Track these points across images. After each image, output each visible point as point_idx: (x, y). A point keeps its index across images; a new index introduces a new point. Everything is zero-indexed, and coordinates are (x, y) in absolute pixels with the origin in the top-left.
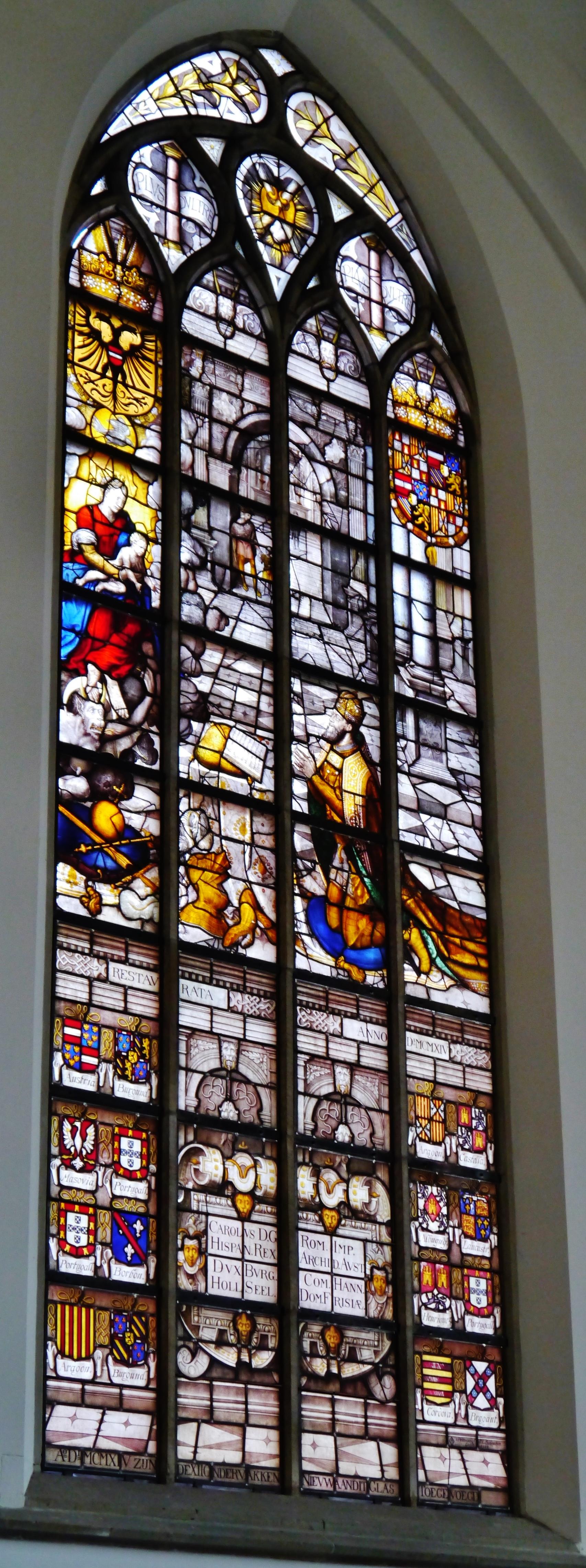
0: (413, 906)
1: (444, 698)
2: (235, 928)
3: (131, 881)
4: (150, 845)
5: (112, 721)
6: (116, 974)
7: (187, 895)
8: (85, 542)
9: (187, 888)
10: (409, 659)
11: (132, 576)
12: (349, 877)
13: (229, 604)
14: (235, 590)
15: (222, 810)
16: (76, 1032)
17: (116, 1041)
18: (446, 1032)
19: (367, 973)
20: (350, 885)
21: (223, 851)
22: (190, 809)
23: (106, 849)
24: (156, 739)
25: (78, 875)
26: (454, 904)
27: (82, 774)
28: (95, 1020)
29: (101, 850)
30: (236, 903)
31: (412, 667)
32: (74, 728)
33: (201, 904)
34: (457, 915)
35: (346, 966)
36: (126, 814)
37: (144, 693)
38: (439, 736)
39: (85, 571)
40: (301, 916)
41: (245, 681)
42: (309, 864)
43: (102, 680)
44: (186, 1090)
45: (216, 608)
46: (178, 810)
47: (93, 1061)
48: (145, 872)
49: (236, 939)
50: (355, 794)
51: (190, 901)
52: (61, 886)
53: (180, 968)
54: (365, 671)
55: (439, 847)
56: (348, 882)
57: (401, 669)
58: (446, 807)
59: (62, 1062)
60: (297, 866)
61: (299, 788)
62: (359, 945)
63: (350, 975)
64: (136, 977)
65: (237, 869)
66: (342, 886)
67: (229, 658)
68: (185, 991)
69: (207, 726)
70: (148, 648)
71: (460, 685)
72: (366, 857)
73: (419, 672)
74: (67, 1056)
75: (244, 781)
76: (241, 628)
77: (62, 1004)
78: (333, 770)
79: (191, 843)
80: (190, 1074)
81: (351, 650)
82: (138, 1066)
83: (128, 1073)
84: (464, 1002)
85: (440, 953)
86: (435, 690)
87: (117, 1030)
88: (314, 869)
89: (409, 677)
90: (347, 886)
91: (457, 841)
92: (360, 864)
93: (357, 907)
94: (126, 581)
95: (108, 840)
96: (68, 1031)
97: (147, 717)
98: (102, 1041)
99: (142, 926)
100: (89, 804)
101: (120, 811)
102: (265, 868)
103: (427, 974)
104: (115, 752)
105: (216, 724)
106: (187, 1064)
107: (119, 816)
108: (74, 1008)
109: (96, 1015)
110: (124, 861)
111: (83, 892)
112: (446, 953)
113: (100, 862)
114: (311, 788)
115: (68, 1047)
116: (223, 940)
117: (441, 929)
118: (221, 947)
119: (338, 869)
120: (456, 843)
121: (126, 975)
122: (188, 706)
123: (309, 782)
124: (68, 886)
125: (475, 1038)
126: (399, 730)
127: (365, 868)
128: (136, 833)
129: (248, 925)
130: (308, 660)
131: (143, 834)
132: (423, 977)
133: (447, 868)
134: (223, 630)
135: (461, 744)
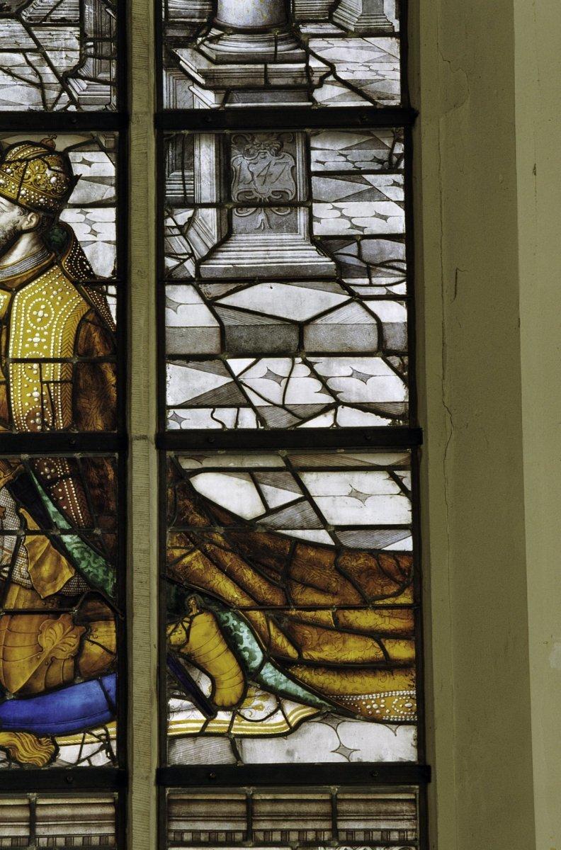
0: (198, 566)
12: (19, 543)
18: (286, 826)
19: (60, 741)
20: (21, 561)
26: (323, 537)
31: (217, 39)
34: (327, 559)
38: (287, 175)
50: (40, 361)
54: (78, 86)
55: (279, 421)
57: (185, 55)
58: (301, 327)
62: (40, 685)
63: (10, 758)
71: (354, 42)
72: (69, 489)
81: (39, 49)
84: (341, 749)
86: (280, 74)
89: (205, 65)
90: (12, 565)
91: (333, 393)
92: (52, 508)
93: (38, 605)
103: (235, 708)
112: (291, 651)
117: (278, 600)
120: (331, 400)
125: (371, 825)
127: (65, 515)
132: (223, 716)
133: (303, 461)
135: (354, 175)
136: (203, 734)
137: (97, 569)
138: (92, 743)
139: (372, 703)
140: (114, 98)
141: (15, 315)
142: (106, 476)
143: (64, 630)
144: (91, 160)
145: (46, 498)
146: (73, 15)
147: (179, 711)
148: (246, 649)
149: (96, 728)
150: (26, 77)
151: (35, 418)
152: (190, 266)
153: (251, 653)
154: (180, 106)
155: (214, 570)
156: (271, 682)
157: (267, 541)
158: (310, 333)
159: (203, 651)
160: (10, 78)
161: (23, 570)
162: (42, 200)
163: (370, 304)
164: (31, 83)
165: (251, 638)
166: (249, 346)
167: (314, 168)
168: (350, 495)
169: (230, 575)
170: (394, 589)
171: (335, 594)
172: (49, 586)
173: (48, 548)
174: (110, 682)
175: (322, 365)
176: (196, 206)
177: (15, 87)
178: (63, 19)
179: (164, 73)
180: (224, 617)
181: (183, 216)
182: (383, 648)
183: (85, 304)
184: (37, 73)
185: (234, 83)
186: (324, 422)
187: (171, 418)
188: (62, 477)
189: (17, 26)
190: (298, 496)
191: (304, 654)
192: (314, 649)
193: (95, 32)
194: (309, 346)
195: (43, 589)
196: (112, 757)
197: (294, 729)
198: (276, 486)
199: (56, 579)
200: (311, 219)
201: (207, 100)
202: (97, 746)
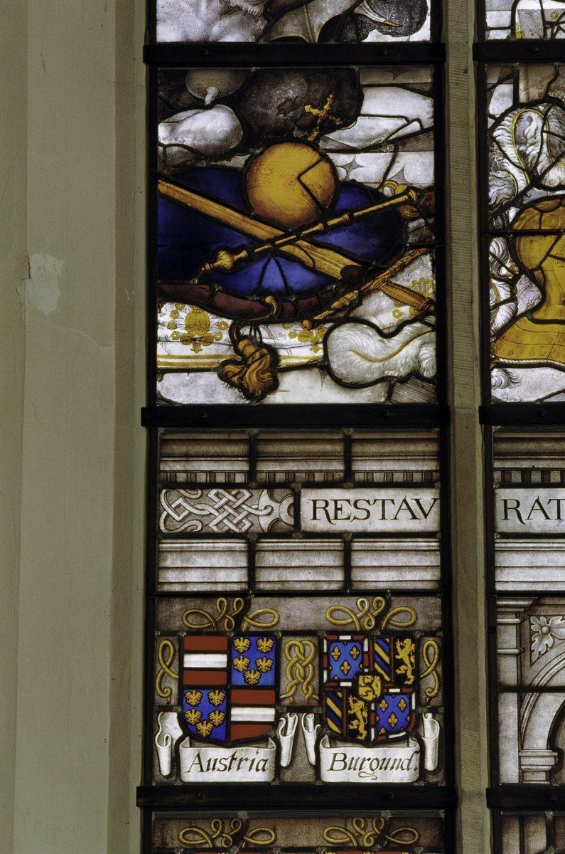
3: (359, 302)
4: (407, 212)
6: (321, 513)
7: (513, 298)
9: (511, 283)
16: (218, 661)
17: (323, 659)
22: (517, 104)
23: (285, 248)
25: (214, 320)
27: (218, 101)
28: (265, 623)
29: (274, 252)
33: (551, 312)
36: (341, 159)
44: (522, 737)
47: (267, 714)
48: (394, 275)
51: (522, 308)
52: (170, 351)
53: (497, 464)
59: (178, 733)
64: (376, 510)
68: (512, 515)
74: (192, 717)
77: (177, 606)
79: (522, 181)
80: (530, 698)
82: (383, 704)
83: (359, 725)
87: (323, 637)
95: (292, 229)
96: (192, 661)
98: (286, 666)
99: (390, 393)
100: (239, 161)
101: (324, 157)
104: (307, 28)
106: (520, 677)
107: (325, 166)
108: (208, 608)
109: (263, 613)
113: (273, 278)
115: (193, 697)
121: (348, 509)
124: (187, 350)
128: (367, 193)
131: (387, 191)
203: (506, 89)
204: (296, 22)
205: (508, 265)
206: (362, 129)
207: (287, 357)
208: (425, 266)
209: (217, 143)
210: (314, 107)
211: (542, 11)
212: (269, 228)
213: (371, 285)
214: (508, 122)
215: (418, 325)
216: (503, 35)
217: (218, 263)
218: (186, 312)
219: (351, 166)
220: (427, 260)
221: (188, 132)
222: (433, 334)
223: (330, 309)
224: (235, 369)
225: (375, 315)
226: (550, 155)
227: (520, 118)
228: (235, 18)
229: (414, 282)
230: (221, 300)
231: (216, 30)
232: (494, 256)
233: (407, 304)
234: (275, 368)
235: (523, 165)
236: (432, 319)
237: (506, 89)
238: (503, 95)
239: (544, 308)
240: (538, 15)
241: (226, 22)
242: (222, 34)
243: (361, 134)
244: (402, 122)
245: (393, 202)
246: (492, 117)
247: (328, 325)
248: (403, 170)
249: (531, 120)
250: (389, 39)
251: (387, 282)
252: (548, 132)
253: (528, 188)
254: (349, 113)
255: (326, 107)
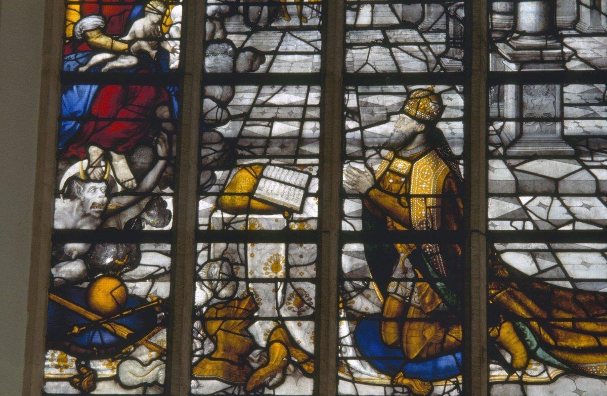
1: (562, 59)
2: (261, 370)
4: (157, 309)
5: (117, 194)
7: (202, 348)
8: (90, 28)
9: (202, 341)
10: (513, 31)
11: (144, 45)
12: (413, 286)
13: (267, 41)
14: (273, 25)
15: (249, 252)
19: (434, 384)
20: (415, 295)
21: (250, 294)
22: (209, 260)
24: (169, 201)
25: (70, 358)
26: (568, 285)
30: (263, 343)
32: (71, 212)
33: (218, 355)
34: (570, 296)
35: (406, 381)
37: (156, 158)
38: (551, 105)
39: (89, 57)
40: (348, 341)
41: (283, 113)
42: (361, 283)
43: (107, 158)
45: (250, 49)
46: (196, 264)
48: (149, 338)
49: (262, 381)
50: (425, 197)
54: (446, 61)
56: (412, 291)
57: (500, 46)
58: (556, 181)
60: (344, 289)
61: (351, 206)
62: (424, 355)
65: (267, 308)
66: (404, 297)
67: (264, 95)
69: (234, 172)
70: (164, 112)
71: (586, 39)
72: (440, 258)
73: (527, 41)
75: (280, 216)
76: (280, 61)
78: (397, 178)
85: (542, 344)
86: (549, 55)
88: (367, 287)
89: (510, 50)
90: (411, 296)
93: (423, 316)
94: (140, 53)
97: (161, 181)
99: (145, 391)
100: (86, 285)
101: (122, 283)
102: (303, 302)
103: (523, 369)
104: (119, 224)
105: (244, 167)
107: (122, 288)
110: (124, 332)
111: (75, 372)
112: (551, 341)
114: (367, 203)
116: (245, 385)
117: (545, 316)
118: (242, 393)
119: (399, 281)
122: (211, 157)
123: (364, 197)
124: (57, 371)
126: (493, 112)
127: (437, 272)
129: (278, 363)
130: (368, 69)
131: (149, 299)
133: (557, 246)
134: (258, 68)
136: (507, 382)
137: (453, 299)
138: (450, 385)
139: (593, 368)
140: (462, 67)
141: (413, 174)
142: (458, 253)
143: (436, 329)
144: (452, 98)
145: (428, 264)
146: (443, 27)
147: (495, 370)
148: (528, 340)
149: (452, 378)
150: (420, 57)
151: (423, 224)
152: (501, 150)
153: (531, 342)
154: (498, 70)
155: (512, 301)
156: (541, 357)
157: (538, 286)
158: (561, 184)
159: (507, 340)
160: (412, 57)
161: (416, 299)
162: (427, 117)
163: (593, 171)
164: (422, 60)
165: (531, 335)
166: (531, 190)
167: (566, 102)
168: (581, 264)
169: (521, 303)
170: (604, 311)
171: (574, 313)
172: (429, 307)
173: (428, 289)
174: (459, 355)
175: (567, 200)
176: (505, 120)
177: (414, 62)
178: (438, 29)
179: (490, 54)
180: (517, 324)
181: (498, 125)
182: (598, 341)
183: (448, 168)
184: (425, 55)
185: (525, 59)
186: (569, 228)
187: (490, 225)
188: (436, 254)
189: (416, 33)
190: (555, 264)
191: (558, 343)
192: (563, 341)
193: (454, 35)
194: (560, 191)
195: (426, 308)
196: (460, 392)
197: (552, 381)
198: (544, 259)
199: (432, 304)
200: (563, 127)
201: (512, 67)
202: (453, 386)
203: (205, 253)
204: (114, 221)
205: (201, 333)
206: (139, 271)
207: (100, 375)
208: (164, 334)
209: (76, 276)
210: (119, 260)
211: (223, 218)
212: (97, 316)
213: (140, 342)
214: (205, 268)
215: (158, 361)
216: (205, 228)
217: (73, 331)
218: (57, 354)
219: (134, 287)
220: (165, 331)
221: (63, 272)
222: (165, 365)
223: (121, 353)
224: (76, 380)
225: (140, 356)
226: (222, 284)
227: (210, 266)
228: (88, 219)
229: (158, 341)
230: (73, 348)
231: (79, 223)
232: (195, 328)
233: (155, 351)
234: (95, 379)
235: (210, 287)
236: (165, 358)
237: (205, 253)
238: (203, 256)
239: (216, 353)
240: (221, 219)
241: (84, 220)
242: (82, 226)
243: (139, 273)
244: (157, 268)
245: (151, 304)
246: (198, 265)
247: (119, 361)
248: (156, 290)
249: (215, 267)
250: (155, 229)
251: (147, 341)
252: (223, 273)
253: (212, 298)
254: (134, 262)
255: (125, 261)
